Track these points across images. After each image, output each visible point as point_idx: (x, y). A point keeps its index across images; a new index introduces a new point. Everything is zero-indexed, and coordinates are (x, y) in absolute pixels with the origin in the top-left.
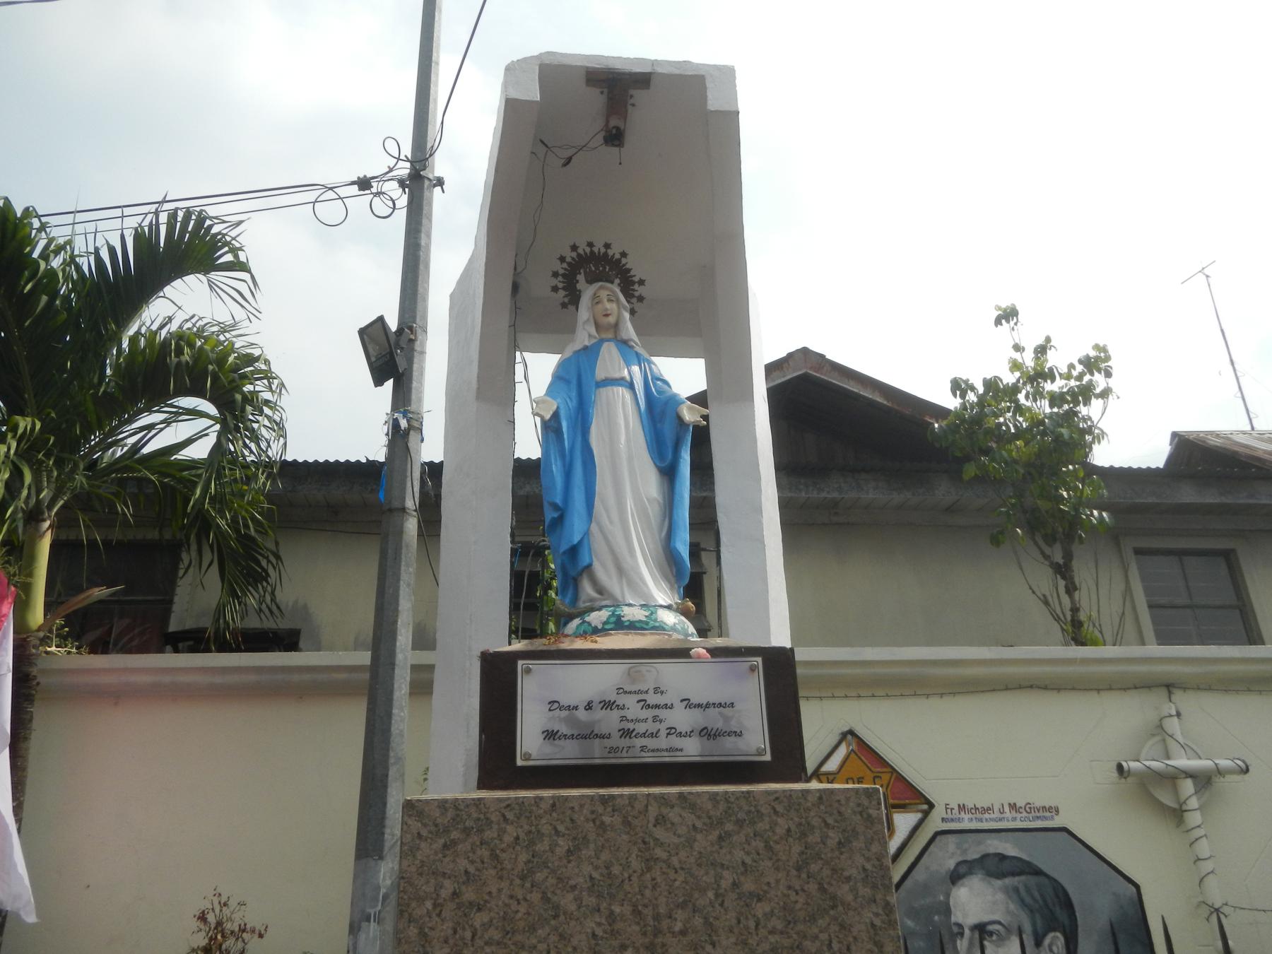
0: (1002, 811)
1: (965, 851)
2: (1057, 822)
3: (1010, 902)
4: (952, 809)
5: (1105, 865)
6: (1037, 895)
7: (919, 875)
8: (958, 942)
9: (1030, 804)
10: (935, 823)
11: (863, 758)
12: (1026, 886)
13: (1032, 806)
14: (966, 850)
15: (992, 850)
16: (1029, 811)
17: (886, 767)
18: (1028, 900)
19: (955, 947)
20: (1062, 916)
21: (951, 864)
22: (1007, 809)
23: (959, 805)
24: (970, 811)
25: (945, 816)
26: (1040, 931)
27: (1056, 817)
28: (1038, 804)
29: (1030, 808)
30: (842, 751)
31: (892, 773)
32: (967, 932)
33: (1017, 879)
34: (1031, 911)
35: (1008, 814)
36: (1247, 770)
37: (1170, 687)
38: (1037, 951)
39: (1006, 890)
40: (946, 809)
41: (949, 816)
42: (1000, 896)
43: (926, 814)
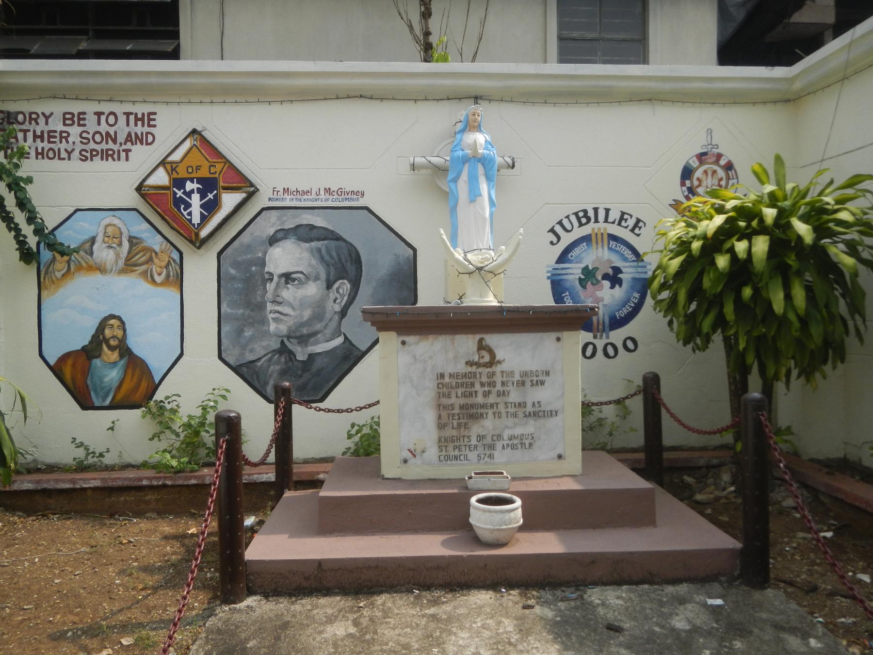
0: (318, 194)
1: (283, 223)
2: (361, 203)
3: (313, 258)
4: (278, 192)
5: (393, 235)
6: (334, 254)
7: (245, 238)
8: (268, 284)
9: (342, 189)
10: (261, 201)
11: (203, 151)
12: (327, 247)
13: (343, 190)
14: (285, 221)
15: (305, 222)
16: (340, 194)
17: (222, 159)
18: (327, 258)
19: (265, 288)
20: (351, 269)
21: (271, 231)
22: (322, 192)
23: (284, 189)
24: (292, 193)
25: (272, 196)
26: (332, 278)
27: (360, 199)
28: (348, 189)
29: (341, 192)
30: (187, 145)
31: (226, 163)
32: (276, 278)
33: (321, 242)
34: (328, 265)
35: (322, 196)
36: (513, 166)
37: (477, 99)
38: (327, 292)
39: (311, 251)
40: (274, 191)
41: (275, 196)
42: (306, 255)
43: (250, 196)
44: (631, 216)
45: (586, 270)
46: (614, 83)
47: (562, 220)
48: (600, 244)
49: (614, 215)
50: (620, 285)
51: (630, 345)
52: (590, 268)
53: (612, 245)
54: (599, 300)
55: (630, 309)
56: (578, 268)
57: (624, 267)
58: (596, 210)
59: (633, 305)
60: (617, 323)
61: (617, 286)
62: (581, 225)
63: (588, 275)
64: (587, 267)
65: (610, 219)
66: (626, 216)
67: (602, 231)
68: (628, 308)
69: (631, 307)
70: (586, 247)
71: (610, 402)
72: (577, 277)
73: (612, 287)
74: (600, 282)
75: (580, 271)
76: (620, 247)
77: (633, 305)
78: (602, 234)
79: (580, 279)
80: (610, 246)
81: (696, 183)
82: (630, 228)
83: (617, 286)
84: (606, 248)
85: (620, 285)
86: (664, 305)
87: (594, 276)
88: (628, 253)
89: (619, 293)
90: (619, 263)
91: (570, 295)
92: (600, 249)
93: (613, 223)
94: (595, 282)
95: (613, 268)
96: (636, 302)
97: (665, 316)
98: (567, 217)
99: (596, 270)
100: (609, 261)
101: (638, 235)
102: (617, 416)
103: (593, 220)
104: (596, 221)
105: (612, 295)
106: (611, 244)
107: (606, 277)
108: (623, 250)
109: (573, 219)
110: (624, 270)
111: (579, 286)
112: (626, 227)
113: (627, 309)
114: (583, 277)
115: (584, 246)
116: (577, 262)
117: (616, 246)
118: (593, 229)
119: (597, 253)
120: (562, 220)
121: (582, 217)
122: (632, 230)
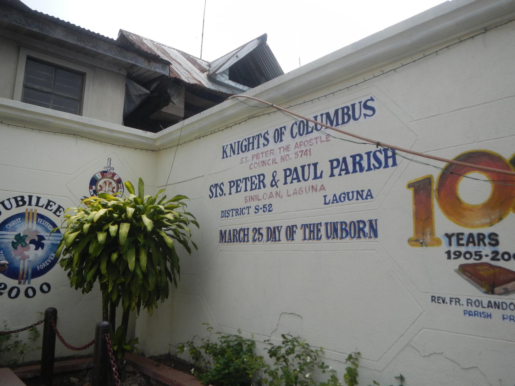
44: (55, 204)
45: (18, 237)
46: (52, 120)
47: (4, 201)
48: (31, 220)
49: (43, 202)
50: (42, 248)
51: (45, 288)
52: (22, 235)
53: (40, 221)
54: (24, 258)
55: (48, 264)
56: (13, 235)
57: (46, 236)
58: (30, 197)
59: (50, 261)
60: (37, 273)
61: (40, 248)
62: (18, 206)
63: (20, 240)
64: (19, 234)
65: (40, 204)
66: (51, 203)
67: (33, 212)
68: (46, 263)
69: (48, 262)
70: (20, 221)
71: (25, 329)
72: (11, 241)
73: (36, 249)
74: (28, 245)
75: (14, 237)
76: (45, 223)
77: (50, 261)
78: (33, 213)
79: (13, 243)
80: (38, 222)
81: (99, 188)
82: (53, 211)
83: (40, 248)
84: (35, 223)
85: (42, 248)
86: (65, 263)
87: (24, 241)
88: (50, 227)
89: (40, 252)
90: (43, 233)
91: (4, 253)
92: (30, 223)
93: (42, 207)
94: (24, 245)
95: (39, 236)
96: (52, 259)
97: (65, 270)
98: (9, 200)
99: (26, 237)
100: (36, 231)
101: (59, 216)
102: (29, 338)
103: (27, 203)
104: (30, 204)
105: (35, 254)
106: (39, 220)
107: (32, 242)
108: (47, 225)
109: (13, 201)
110: (46, 238)
111: (12, 247)
112: (51, 210)
113: (46, 264)
114: (15, 241)
115: (19, 220)
116: (12, 231)
117: (42, 222)
118: (27, 210)
119: (28, 225)
120: (4, 201)
121: (20, 201)
122: (55, 213)
